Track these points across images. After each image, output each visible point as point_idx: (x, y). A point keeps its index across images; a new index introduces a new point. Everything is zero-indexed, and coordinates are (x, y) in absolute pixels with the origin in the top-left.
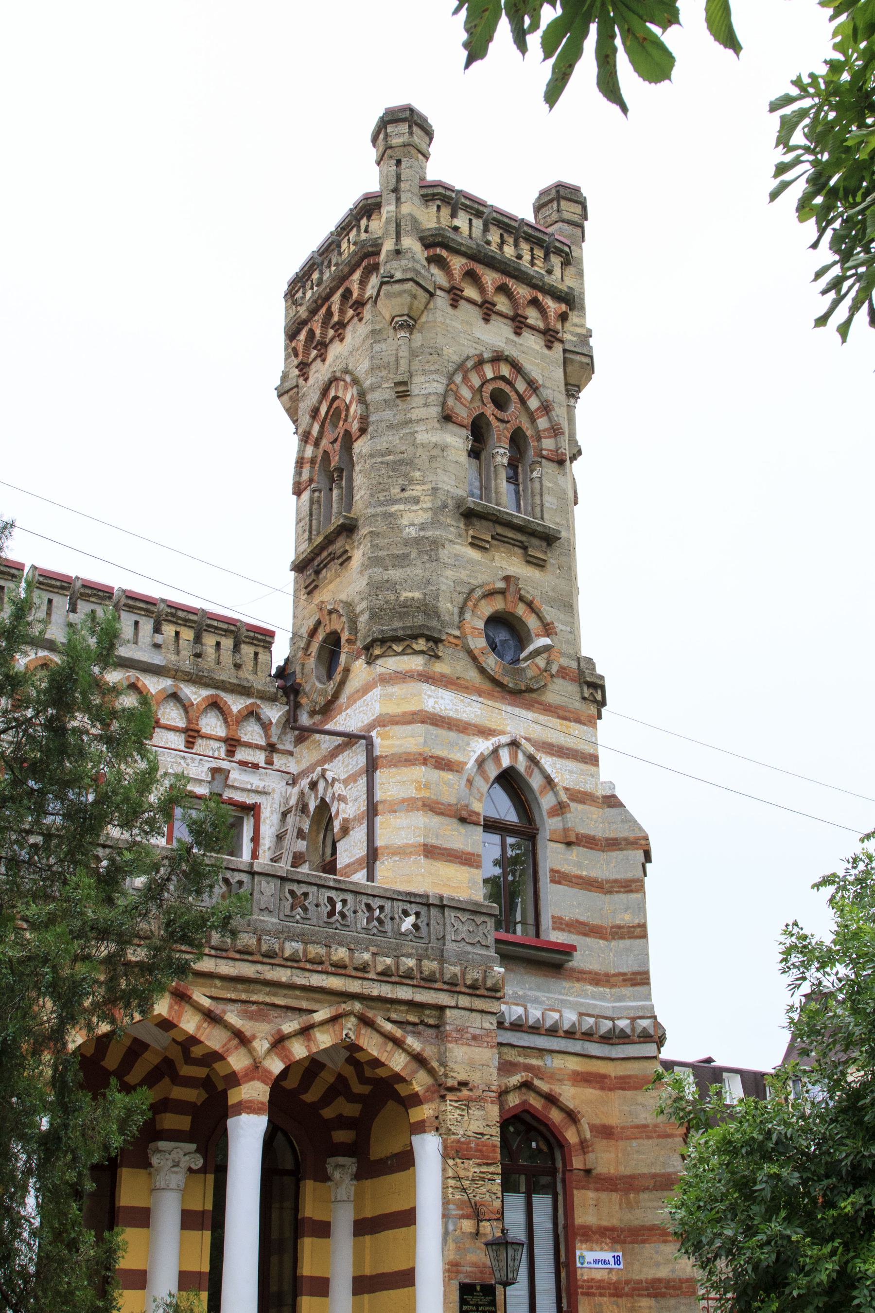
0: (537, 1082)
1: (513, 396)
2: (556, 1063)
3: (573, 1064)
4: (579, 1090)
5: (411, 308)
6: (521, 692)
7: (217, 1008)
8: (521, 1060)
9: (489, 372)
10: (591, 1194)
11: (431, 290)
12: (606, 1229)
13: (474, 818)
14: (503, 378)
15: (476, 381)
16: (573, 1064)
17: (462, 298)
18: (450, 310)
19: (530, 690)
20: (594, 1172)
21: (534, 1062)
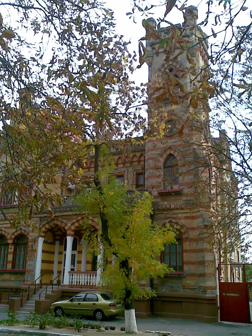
0: (173, 220)
1: (174, 67)
2: (180, 215)
3: (184, 215)
4: (186, 220)
5: (149, 62)
6: (171, 136)
7: (93, 219)
8: (171, 216)
9: (166, 66)
10: (188, 243)
11: (152, 56)
12: (192, 250)
13: (160, 167)
14: (171, 65)
15: (163, 70)
16: (184, 215)
17: (160, 53)
18: (157, 57)
19: (175, 134)
20: (189, 238)
21: (174, 216)
